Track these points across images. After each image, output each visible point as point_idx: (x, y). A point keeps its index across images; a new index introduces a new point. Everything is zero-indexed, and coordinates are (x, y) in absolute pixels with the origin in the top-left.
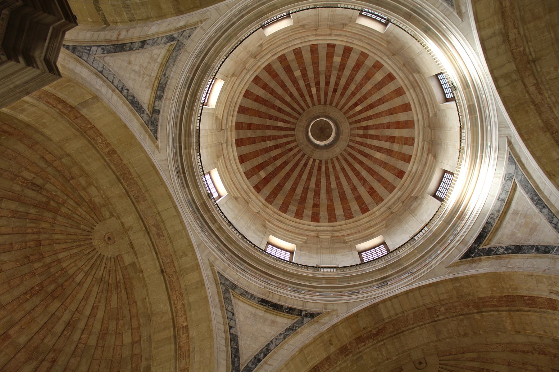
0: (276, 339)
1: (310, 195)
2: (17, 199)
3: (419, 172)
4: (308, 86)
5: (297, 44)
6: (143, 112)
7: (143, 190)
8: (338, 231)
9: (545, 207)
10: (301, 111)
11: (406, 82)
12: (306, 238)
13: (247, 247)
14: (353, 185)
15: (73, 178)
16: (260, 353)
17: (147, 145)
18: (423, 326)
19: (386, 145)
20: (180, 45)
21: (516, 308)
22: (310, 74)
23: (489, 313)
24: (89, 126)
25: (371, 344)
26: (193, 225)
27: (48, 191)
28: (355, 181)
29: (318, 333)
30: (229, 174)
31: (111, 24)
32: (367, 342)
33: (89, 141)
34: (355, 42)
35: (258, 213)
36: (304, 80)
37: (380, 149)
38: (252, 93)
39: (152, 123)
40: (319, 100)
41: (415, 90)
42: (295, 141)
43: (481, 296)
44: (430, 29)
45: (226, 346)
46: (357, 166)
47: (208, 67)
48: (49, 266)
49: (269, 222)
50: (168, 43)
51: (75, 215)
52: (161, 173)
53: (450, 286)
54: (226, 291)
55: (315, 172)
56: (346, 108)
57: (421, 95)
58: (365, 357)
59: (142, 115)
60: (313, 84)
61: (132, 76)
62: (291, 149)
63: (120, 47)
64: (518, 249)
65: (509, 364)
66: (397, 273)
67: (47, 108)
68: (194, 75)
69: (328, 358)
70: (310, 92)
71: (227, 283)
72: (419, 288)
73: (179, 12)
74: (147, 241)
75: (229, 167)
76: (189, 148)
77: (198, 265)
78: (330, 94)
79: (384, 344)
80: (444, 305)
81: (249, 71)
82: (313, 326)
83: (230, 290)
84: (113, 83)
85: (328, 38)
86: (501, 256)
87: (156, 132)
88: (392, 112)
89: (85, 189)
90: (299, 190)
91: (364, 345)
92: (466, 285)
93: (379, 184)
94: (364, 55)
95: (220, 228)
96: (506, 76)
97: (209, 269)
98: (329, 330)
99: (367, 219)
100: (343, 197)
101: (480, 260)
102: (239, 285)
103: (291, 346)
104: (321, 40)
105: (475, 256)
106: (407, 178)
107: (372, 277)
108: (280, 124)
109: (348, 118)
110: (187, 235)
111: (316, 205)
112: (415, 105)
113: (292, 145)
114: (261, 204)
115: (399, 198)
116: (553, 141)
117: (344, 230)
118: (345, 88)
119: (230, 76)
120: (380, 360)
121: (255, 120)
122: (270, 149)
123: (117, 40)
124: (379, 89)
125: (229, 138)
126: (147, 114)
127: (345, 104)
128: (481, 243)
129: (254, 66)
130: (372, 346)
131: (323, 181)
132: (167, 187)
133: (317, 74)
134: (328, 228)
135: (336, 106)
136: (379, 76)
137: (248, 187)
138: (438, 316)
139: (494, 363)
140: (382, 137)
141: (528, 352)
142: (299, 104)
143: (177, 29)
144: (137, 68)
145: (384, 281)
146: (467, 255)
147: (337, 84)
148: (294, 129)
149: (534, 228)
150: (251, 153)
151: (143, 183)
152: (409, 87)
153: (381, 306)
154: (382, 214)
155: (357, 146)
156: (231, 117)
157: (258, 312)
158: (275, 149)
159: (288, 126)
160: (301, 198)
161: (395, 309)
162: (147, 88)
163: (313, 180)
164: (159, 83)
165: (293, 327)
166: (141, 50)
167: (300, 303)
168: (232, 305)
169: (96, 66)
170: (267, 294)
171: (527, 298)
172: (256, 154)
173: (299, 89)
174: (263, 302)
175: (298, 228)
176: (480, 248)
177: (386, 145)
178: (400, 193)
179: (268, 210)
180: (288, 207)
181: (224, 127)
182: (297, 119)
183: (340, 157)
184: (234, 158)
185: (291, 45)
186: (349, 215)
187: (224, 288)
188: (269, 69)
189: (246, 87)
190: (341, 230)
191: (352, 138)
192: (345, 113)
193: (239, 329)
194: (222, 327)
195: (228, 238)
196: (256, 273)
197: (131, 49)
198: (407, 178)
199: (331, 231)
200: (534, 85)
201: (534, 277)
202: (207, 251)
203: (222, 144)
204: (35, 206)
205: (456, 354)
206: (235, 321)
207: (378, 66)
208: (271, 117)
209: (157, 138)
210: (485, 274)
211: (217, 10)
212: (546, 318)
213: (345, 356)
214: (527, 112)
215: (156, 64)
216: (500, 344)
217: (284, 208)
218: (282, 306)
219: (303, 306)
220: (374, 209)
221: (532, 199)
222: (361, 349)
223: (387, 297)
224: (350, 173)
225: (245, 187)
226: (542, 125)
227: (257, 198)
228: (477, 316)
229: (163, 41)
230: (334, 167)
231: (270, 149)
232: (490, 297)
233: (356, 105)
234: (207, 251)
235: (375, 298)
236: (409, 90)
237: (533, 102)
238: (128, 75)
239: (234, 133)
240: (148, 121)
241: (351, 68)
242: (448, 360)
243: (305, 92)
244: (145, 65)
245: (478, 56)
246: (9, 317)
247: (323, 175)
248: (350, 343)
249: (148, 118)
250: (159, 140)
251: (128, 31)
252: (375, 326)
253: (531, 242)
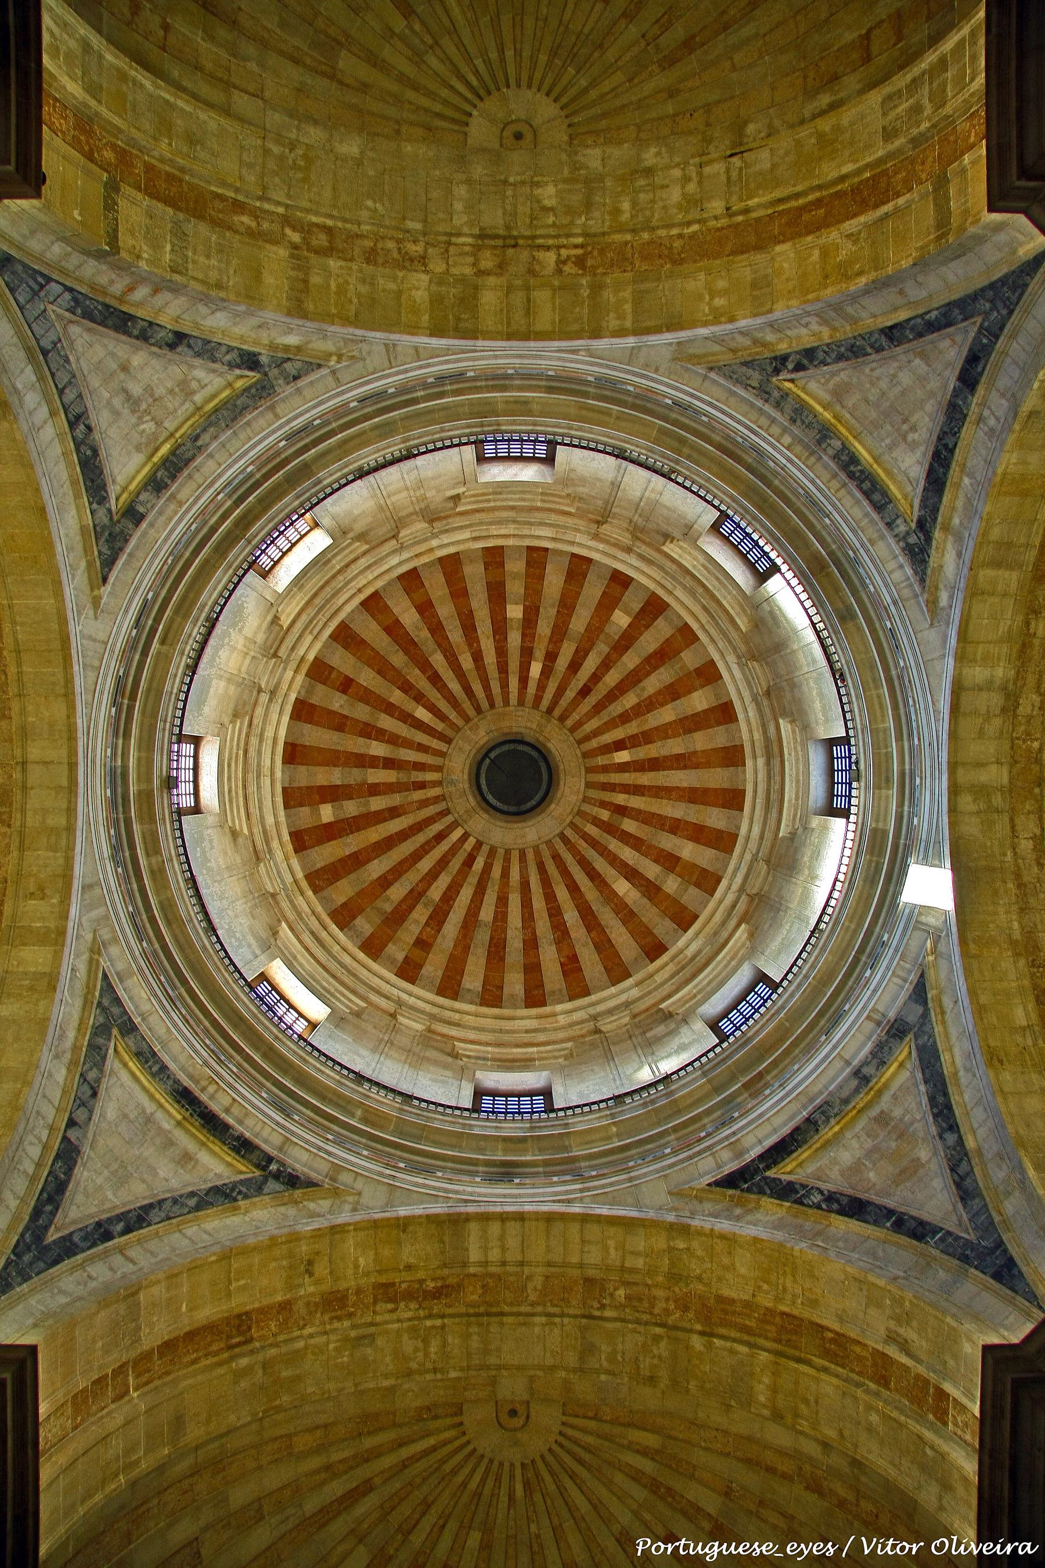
0: (175, 1201)
1: (420, 914)
3: (701, 960)
4: (527, 654)
5: (542, 536)
6: (103, 500)
7: (13, 690)
8: (450, 1023)
9: (953, 1127)
10: (485, 704)
11: (757, 736)
12: (364, 1005)
13: (204, 947)
14: (534, 933)
16: (119, 1218)
17: (74, 584)
18: (557, 1320)
19: (651, 870)
20: (264, 388)
21: (797, 1353)
22: (544, 628)
23: (728, 1344)
25: (410, 1314)
26: (97, 832)
28: (543, 925)
29: (286, 1230)
30: (245, 772)
31: (123, 254)
32: (402, 1305)
34: (679, 593)
35: (273, 896)
36: (524, 635)
37: (631, 874)
38: (387, 607)
39: (112, 538)
40: (538, 699)
41: (768, 763)
42: (439, 769)
43: (726, 1292)
44: (853, 617)
45: (39, 1165)
46: (562, 894)
47: (306, 470)
49: (292, 929)
50: (238, 367)
52: (76, 668)
53: (660, 1242)
54: (102, 1030)
55: (456, 864)
56: (594, 743)
57: (778, 778)
58: (380, 1342)
59: (95, 506)
60: (540, 653)
61: (117, 402)
62: (422, 786)
63: (118, 320)
64: (855, 1208)
65: (727, 1494)
66: (546, 1163)
68: (266, 477)
69: (285, 1307)
70: (525, 668)
71: (116, 1010)
72: (585, 1219)
73: (297, 309)
75: (252, 753)
76: (173, 645)
77: (62, 932)
78: (570, 694)
79: (443, 1327)
80: (627, 1284)
81: (402, 548)
82: (282, 1209)
83: (115, 1032)
84: (61, 392)
85: (621, 555)
86: (810, 1211)
87: (109, 563)
88: (695, 796)
90: (397, 892)
91: (392, 1311)
92: (699, 1253)
93: (596, 957)
94: (686, 635)
95: (159, 874)
96: (981, 791)
97: (86, 956)
98: (317, 1235)
99: (533, 1024)
100: (497, 951)
101: (758, 1207)
102: (143, 1028)
103: (205, 1237)
104: (604, 553)
105: (749, 1190)
106: (666, 964)
107: (481, 1150)
108: (422, 714)
109: (589, 770)
110: (70, 848)
111: (423, 944)
112: (755, 797)
113: (430, 776)
114: (289, 879)
115: (627, 1004)
116: (1026, 983)
117: (464, 1027)
118: (612, 696)
119: (351, 535)
120: (414, 1365)
121: (367, 678)
122: (373, 762)
123: (121, 300)
124: (689, 731)
125: (284, 686)
126: (110, 511)
127: (596, 733)
128: (776, 1163)
129: (419, 542)
130: (410, 1320)
131: (466, 894)
132: (74, 707)
133: (559, 632)
134: (428, 1008)
135: (573, 730)
136: (699, 701)
137: (277, 823)
138: (603, 1307)
139: (692, 1477)
140: (650, 847)
141: (784, 1476)
142: (487, 687)
143: (273, 347)
144: (136, 389)
145: (505, 1172)
146: (730, 1181)
147: (596, 677)
148: (448, 741)
149: (910, 1170)
150: (320, 750)
151: (20, 673)
152: (759, 752)
153: (474, 1227)
154: (572, 1025)
155: (582, 845)
156: (309, 638)
157: (160, 1115)
158: (385, 767)
159: (440, 726)
160: (395, 910)
161: (504, 1249)
162: (138, 448)
163: (443, 881)
164: (173, 452)
165: (233, 1190)
166: (166, 351)
167: (277, 1139)
168: (101, 1071)
170: (204, 1083)
171: (830, 1335)
172: (333, 758)
173: (501, 652)
174: (184, 1097)
175: (354, 975)
176: (768, 1174)
177: (651, 870)
178: (635, 993)
179: (300, 901)
180: (354, 917)
181: (283, 652)
182: (467, 719)
183: (530, 856)
184: (275, 740)
185: (526, 532)
186: (492, 996)
187: (101, 1020)
188: (451, 566)
189: (379, 584)
190: (458, 1025)
191: (578, 821)
192: (586, 755)
193: (90, 1136)
194: (50, 1113)
195: (168, 906)
196: (199, 1022)
197: (144, 337)
198: (666, 964)
199: (433, 1017)
200: (1034, 838)
201: (865, 1287)
202: (100, 911)
203: (260, 690)
205: (611, 1422)
206: (91, 1112)
207: (708, 674)
208: (406, 687)
209: (105, 580)
210: (756, 1240)
211: (390, 349)
212: (856, 1399)
213: (332, 1319)
214: (996, 892)
215: (187, 405)
216: (726, 1432)
217: (343, 916)
218: (227, 1127)
219: (280, 1149)
220: (559, 1008)
221: (932, 1099)
222: (379, 1318)
223: (498, 1209)
224: (539, 903)
225: (270, 820)
226: (1017, 935)
227: (287, 859)
228: (697, 1342)
229: (228, 357)
230: (505, 874)
231: (373, 762)
232: (747, 1304)
233: (620, 745)
234: (100, 911)
235: (466, 1201)
236: (755, 757)
237: (1018, 875)
238: (106, 395)
239: (300, 678)
240: (104, 527)
241: (645, 654)
242: (584, 1431)
243: (514, 665)
244: (160, 391)
245: (936, 720)
247: (473, 879)
248: (359, 1291)
249: (106, 520)
250: (108, 587)
251: (156, 291)
252: (438, 1272)
253: (891, 1203)
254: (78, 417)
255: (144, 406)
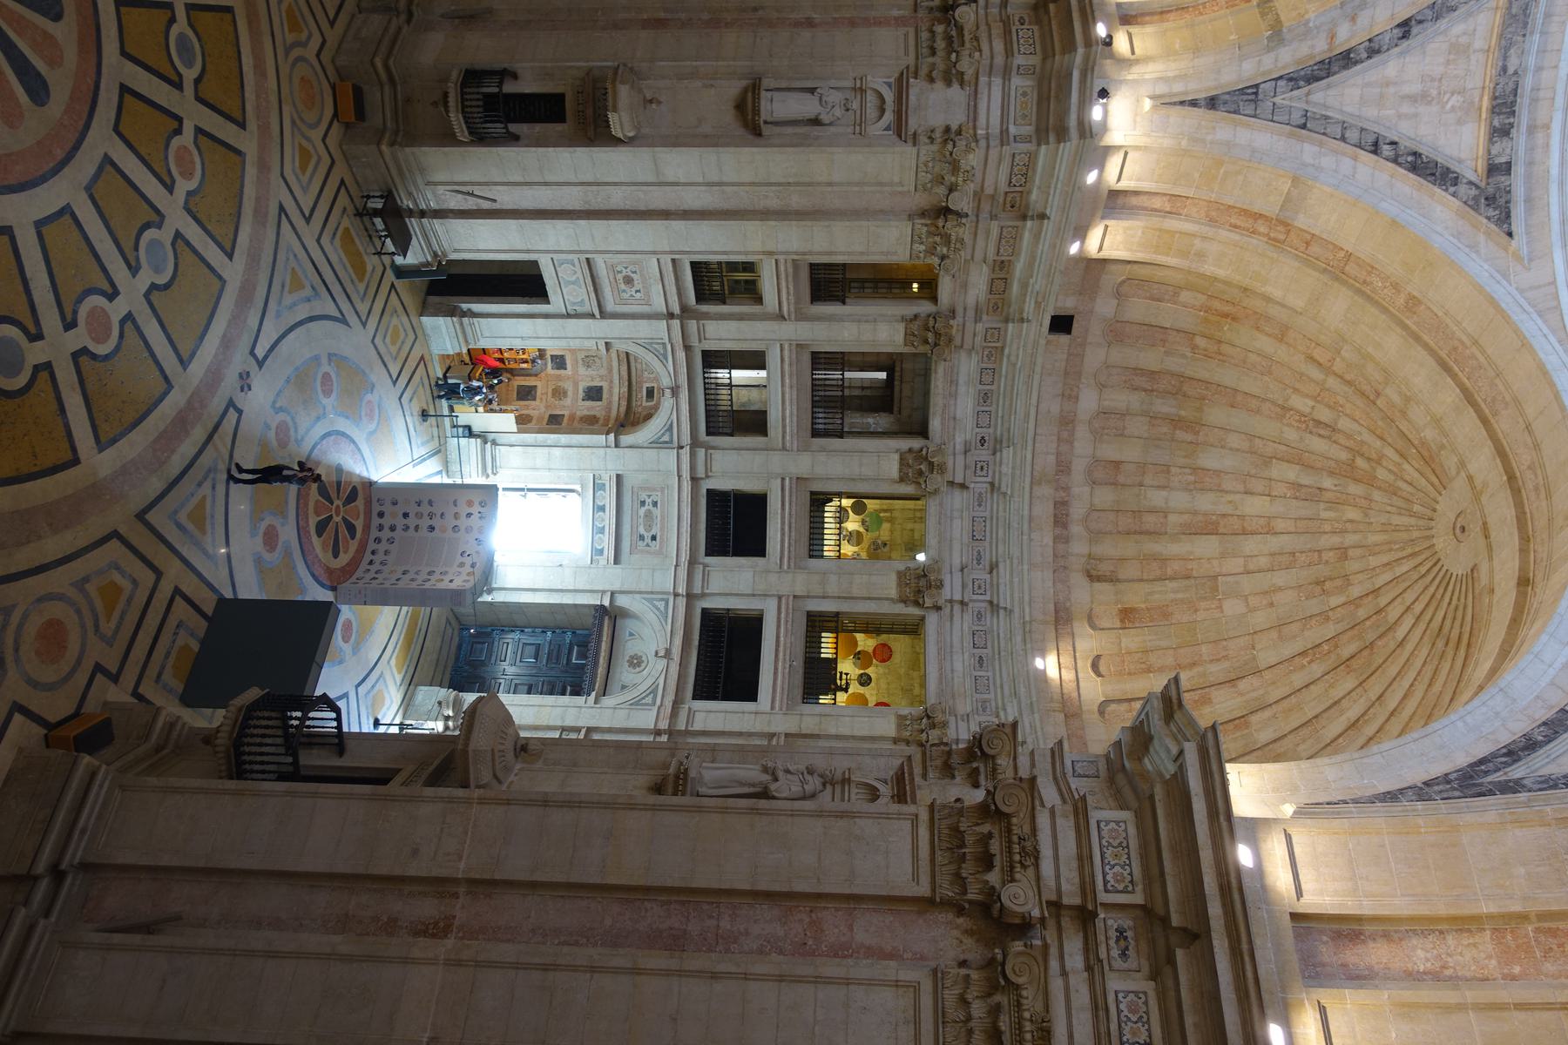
2: (1298, 459)
6: (1456, 181)
15: (1378, 394)
24: (1342, 254)
27: (1349, 437)
33: (1359, 292)
39: (1491, 200)
48: (1355, 603)
51: (1401, 484)
59: (1452, 189)
61: (1406, 108)
63: (1346, 59)
67: (1237, 237)
74: (1510, 513)
84: (1343, 139)
89: (1404, 413)
123: (1330, 50)
126: (1471, 183)
144: (1415, 88)
162: (1460, 122)
166: (1405, 44)
169: (1285, 118)
204: (1331, 473)
209: (1510, 234)
240: (1476, 198)
246: (1261, 692)
249: (1474, 192)
251: (1353, 19)
254: (1376, 144)
255: (1434, 92)
